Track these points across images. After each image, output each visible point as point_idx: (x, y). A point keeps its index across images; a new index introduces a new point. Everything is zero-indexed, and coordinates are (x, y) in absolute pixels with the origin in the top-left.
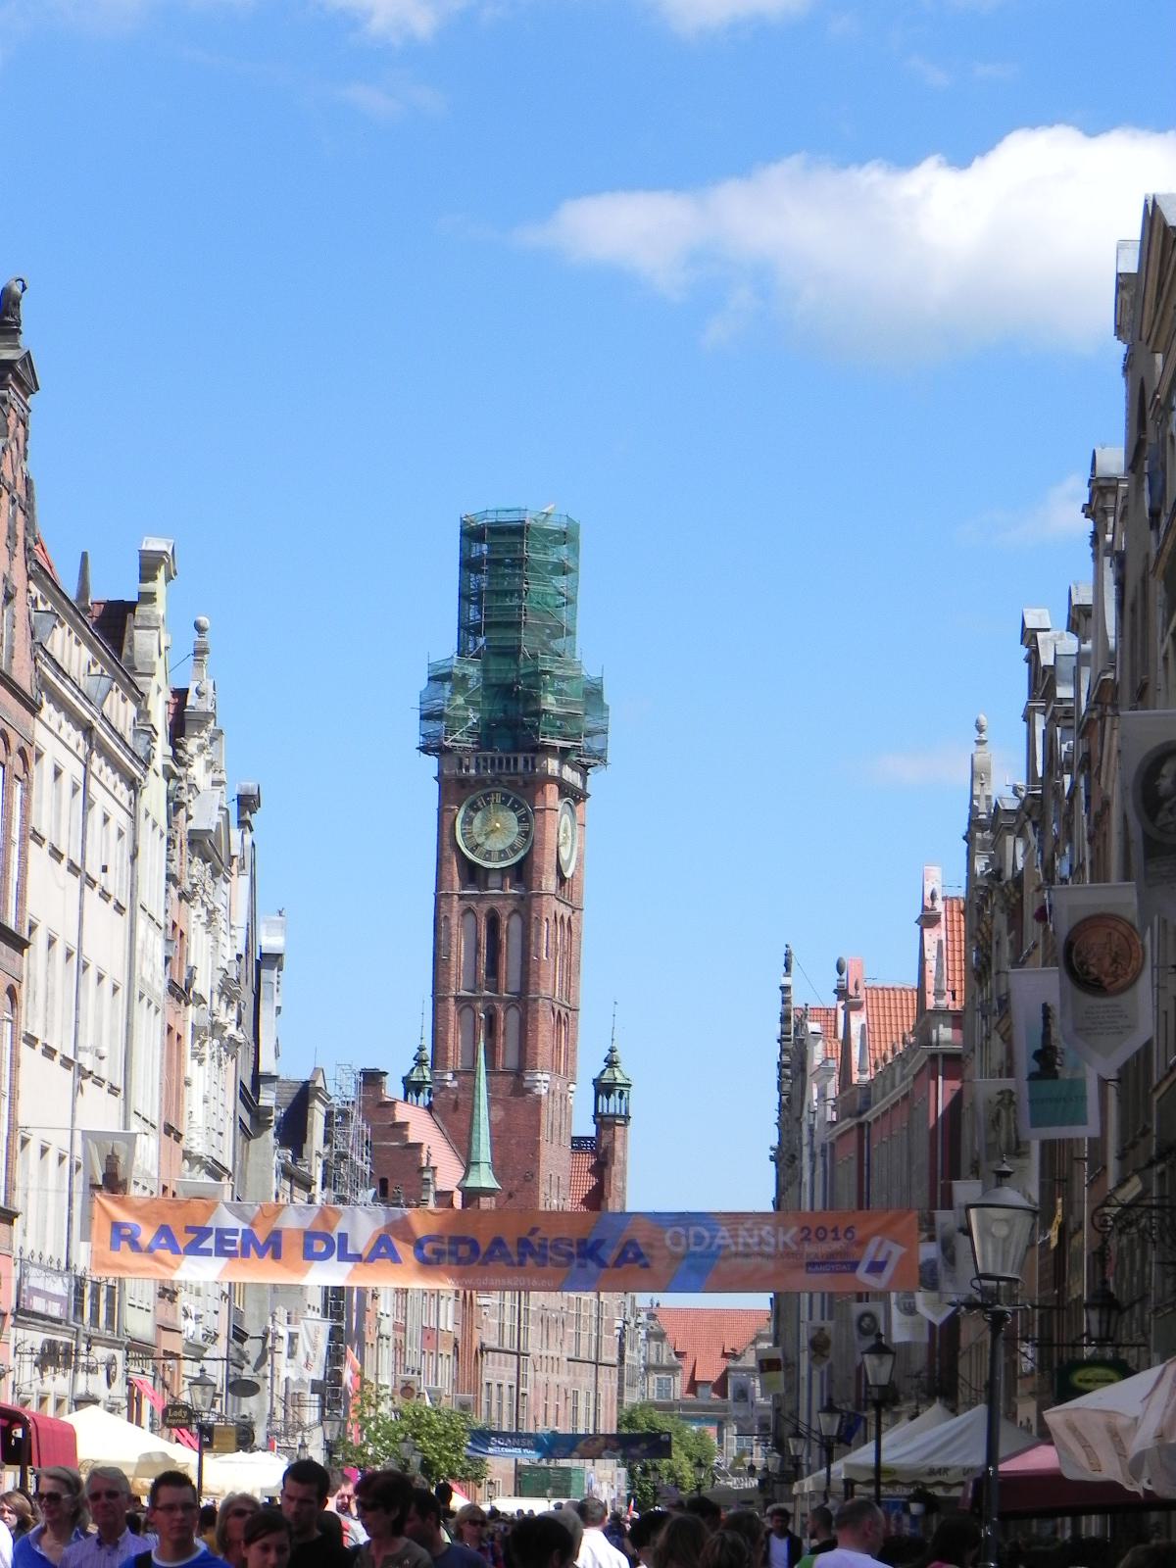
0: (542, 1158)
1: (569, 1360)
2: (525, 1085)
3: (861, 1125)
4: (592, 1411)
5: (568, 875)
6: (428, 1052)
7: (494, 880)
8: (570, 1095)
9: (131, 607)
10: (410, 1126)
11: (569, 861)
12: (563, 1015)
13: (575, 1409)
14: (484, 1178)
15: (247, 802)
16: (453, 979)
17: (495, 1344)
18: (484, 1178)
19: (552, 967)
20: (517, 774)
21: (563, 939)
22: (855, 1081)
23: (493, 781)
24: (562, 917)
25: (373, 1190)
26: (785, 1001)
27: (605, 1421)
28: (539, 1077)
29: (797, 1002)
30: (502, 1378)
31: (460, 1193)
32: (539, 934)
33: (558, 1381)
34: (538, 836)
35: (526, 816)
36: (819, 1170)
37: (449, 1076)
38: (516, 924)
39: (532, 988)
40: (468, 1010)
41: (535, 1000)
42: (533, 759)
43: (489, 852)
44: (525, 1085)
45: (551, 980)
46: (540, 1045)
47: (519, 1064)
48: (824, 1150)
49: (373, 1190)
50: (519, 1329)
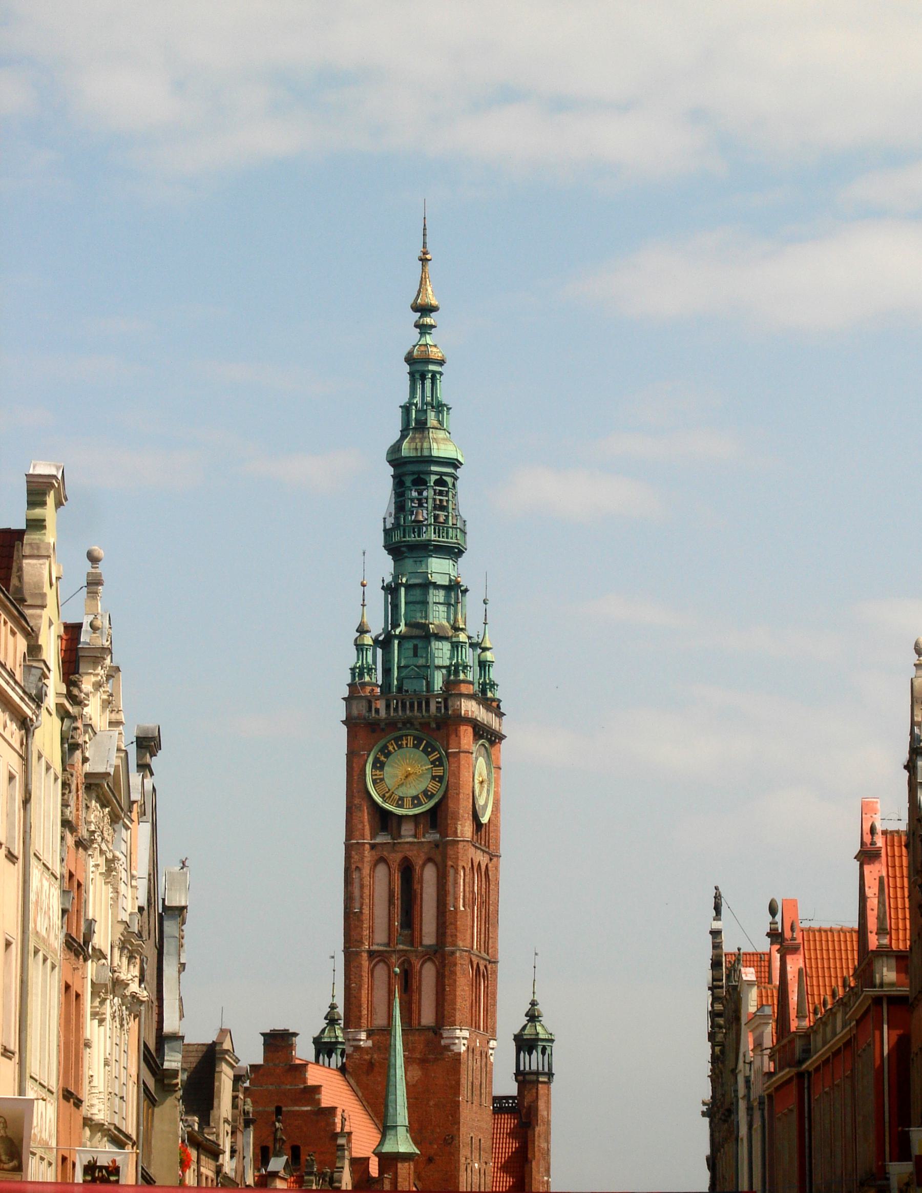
0: (462, 1121)
2: (443, 1042)
3: (800, 1075)
5: (484, 820)
6: (340, 1010)
7: (407, 830)
8: (491, 1051)
9: (18, 535)
10: (323, 1089)
11: (486, 805)
12: (482, 968)
14: (402, 1143)
15: (148, 744)
16: (366, 933)
18: (402, 1143)
19: (469, 918)
20: (430, 717)
21: (480, 888)
22: (793, 1029)
23: (404, 724)
25: (285, 1157)
26: (717, 946)
28: (458, 1033)
29: (729, 946)
31: (377, 1159)
32: (456, 883)
34: (452, 780)
35: (439, 759)
36: (757, 1124)
37: (363, 1036)
38: (429, 874)
39: (449, 939)
40: (381, 965)
41: (453, 953)
43: (401, 799)
44: (443, 1042)
45: (469, 931)
46: (459, 1000)
48: (761, 1103)
49: (285, 1157)
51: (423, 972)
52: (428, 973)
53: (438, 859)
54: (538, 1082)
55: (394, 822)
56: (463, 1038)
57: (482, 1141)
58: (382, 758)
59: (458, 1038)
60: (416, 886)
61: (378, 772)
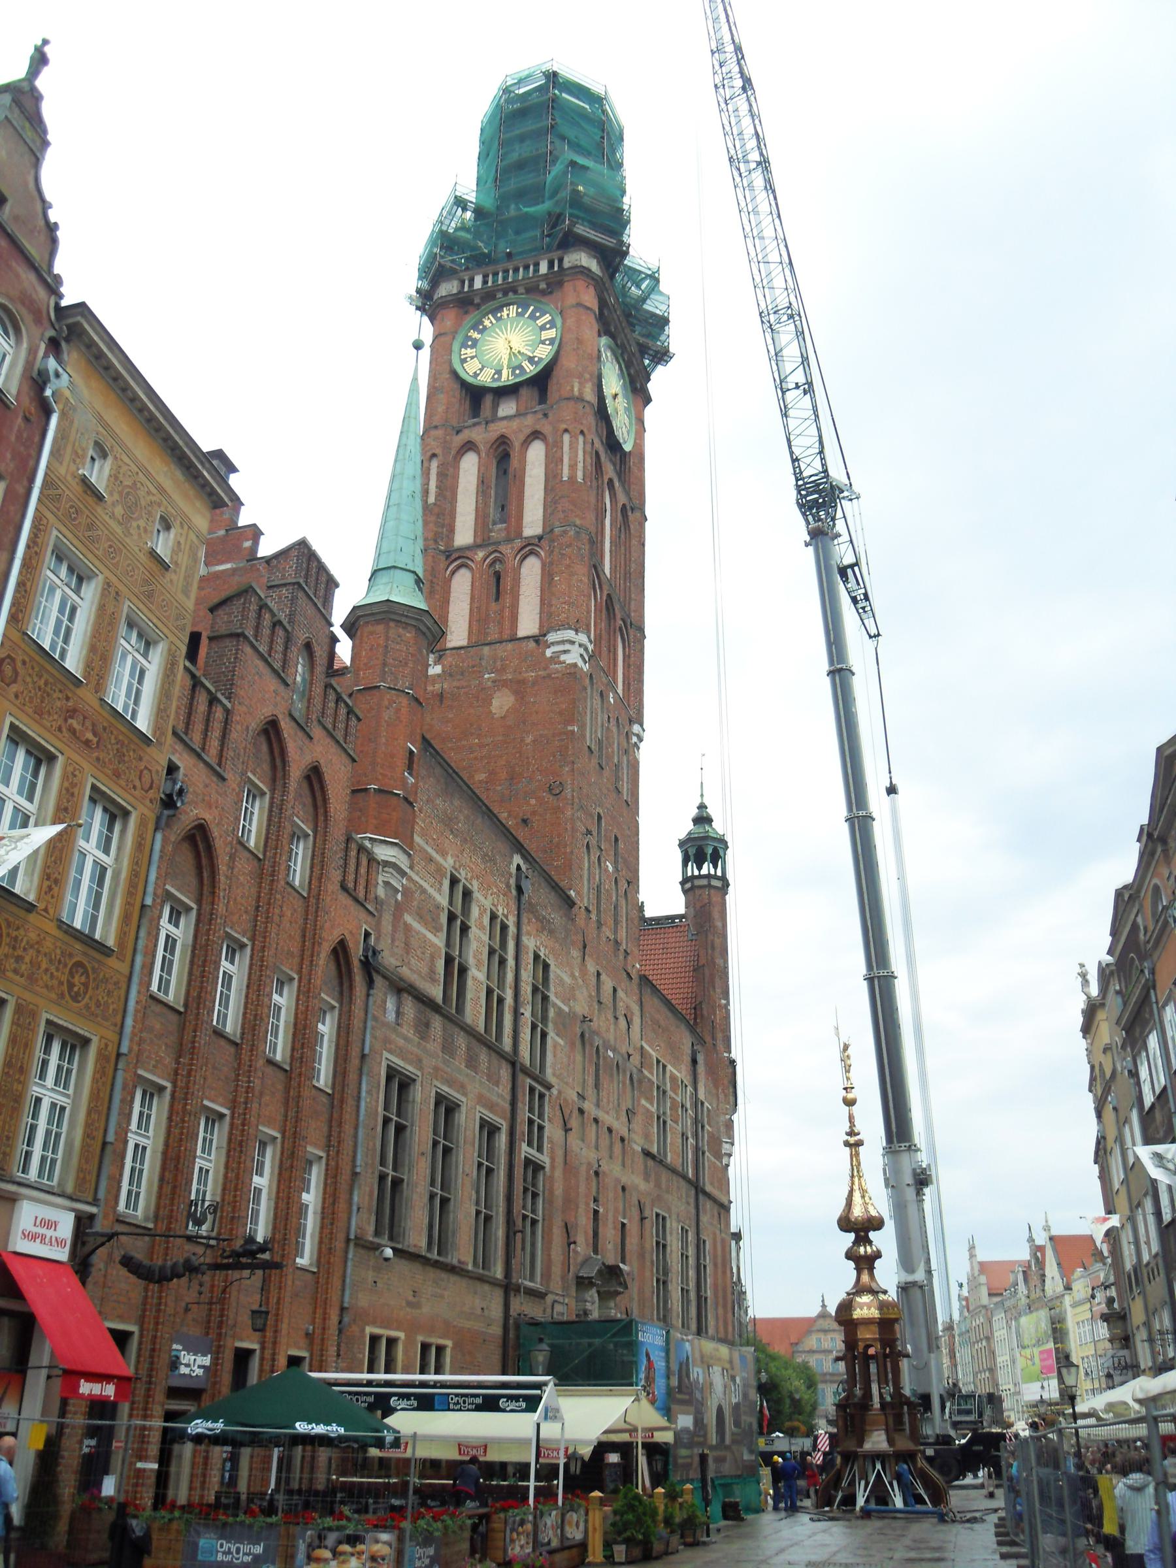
1: (647, 1154)
2: (548, 653)
4: (692, 1261)
7: (507, 408)
8: (635, 739)
13: (661, 1247)
17: (437, 992)
24: (611, 481)
27: (715, 1286)
30: (462, 1088)
33: (624, 1180)
40: (463, 571)
42: (561, 260)
44: (548, 653)
47: (541, 626)
50: (517, 1014)
51: (522, 570)
52: (531, 572)
53: (547, 429)
54: (709, 886)
55: (488, 400)
56: (580, 645)
57: (621, 845)
58: (476, 335)
59: (573, 643)
60: (514, 462)
61: (469, 351)
